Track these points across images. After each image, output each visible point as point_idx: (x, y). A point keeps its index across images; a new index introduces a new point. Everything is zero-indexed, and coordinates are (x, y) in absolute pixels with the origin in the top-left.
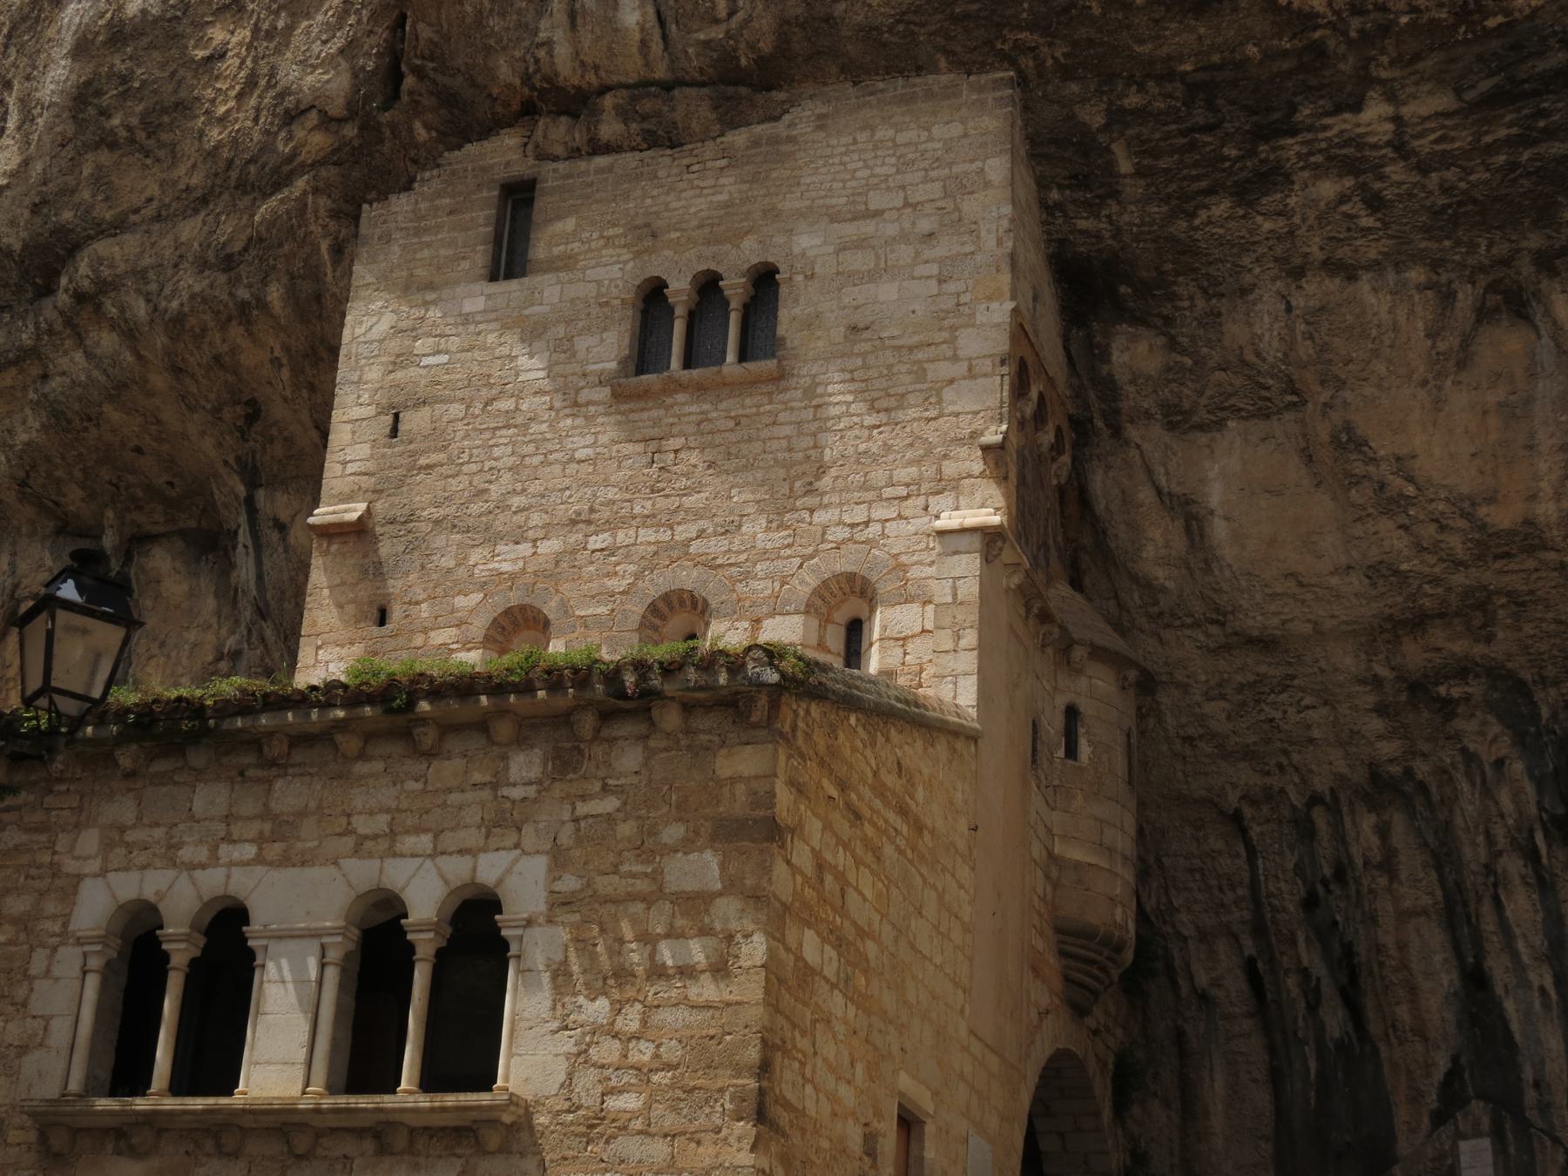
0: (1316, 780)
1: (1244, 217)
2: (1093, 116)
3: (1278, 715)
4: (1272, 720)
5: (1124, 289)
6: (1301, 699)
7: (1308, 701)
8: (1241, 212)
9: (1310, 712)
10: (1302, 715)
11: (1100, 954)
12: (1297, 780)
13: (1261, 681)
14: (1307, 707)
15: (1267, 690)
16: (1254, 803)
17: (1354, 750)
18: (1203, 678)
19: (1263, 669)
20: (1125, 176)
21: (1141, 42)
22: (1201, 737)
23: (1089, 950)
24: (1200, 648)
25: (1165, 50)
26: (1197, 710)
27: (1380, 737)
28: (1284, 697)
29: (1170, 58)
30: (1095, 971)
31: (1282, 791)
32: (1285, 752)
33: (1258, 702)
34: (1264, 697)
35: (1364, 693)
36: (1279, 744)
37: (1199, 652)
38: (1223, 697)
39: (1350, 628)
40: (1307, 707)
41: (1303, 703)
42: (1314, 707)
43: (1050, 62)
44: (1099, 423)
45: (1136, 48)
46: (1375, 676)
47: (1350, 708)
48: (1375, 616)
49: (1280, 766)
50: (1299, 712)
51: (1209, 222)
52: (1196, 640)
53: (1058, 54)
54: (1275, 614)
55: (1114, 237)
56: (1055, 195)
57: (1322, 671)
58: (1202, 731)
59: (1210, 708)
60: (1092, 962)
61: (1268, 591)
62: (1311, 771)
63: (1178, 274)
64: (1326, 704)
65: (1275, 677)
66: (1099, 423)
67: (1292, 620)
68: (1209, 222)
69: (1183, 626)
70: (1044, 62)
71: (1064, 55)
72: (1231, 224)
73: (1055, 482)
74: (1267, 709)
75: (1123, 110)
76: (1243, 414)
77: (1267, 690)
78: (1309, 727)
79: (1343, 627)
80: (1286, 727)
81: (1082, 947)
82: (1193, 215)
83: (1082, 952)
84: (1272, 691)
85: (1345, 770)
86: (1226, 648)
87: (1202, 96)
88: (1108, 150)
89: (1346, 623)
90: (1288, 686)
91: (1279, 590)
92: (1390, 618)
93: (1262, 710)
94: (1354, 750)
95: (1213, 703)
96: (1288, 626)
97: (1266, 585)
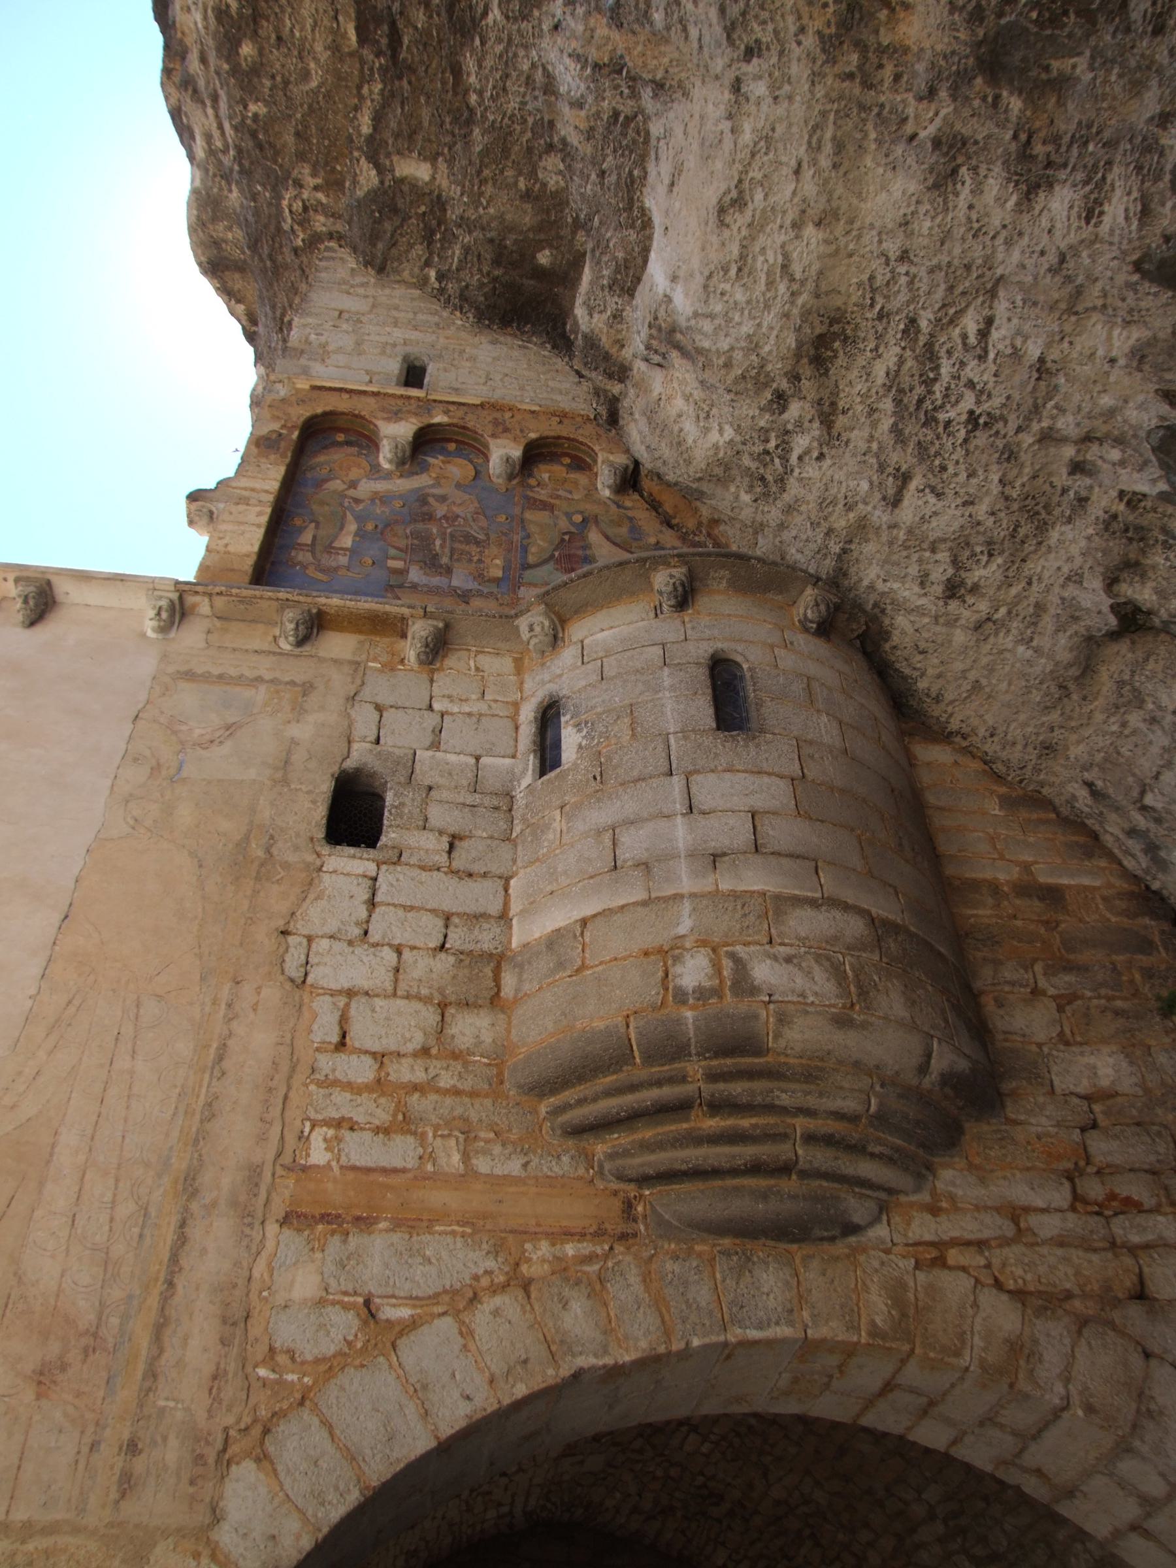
0: (1132, 414)
1: (483, 43)
2: (368, 177)
3: (969, 402)
4: (973, 418)
5: (544, 258)
6: (964, 337)
7: (971, 324)
8: (477, 42)
9: (995, 335)
10: (991, 356)
11: (683, 1079)
12: (1115, 454)
13: (901, 391)
14: (984, 334)
15: (920, 390)
16: (1131, 567)
17: (1096, 290)
18: (865, 485)
19: (880, 371)
20: (433, 178)
21: (306, 75)
22: (955, 562)
23: (633, 1088)
24: (821, 457)
25: (325, 56)
26: (902, 535)
27: (1091, 213)
28: (946, 369)
29: (335, 48)
30: (712, 1124)
31: (1133, 500)
32: (1048, 437)
33: (930, 421)
34: (927, 405)
35: (977, 191)
36: (1027, 439)
37: (828, 462)
38: (905, 478)
39: (828, 148)
40: (984, 334)
41: (972, 340)
42: (989, 321)
43: (321, 196)
44: (616, 388)
45: (314, 84)
46: (937, 143)
47: (1008, 243)
48: (816, 77)
49: (1077, 468)
50: (982, 358)
51: (480, 93)
52: (807, 452)
53: (311, 182)
54: (770, 284)
55: (470, 233)
56: (433, 274)
57: (904, 257)
58: (943, 556)
59: (907, 513)
60: (679, 1108)
61: (733, 272)
62: (1111, 413)
63: (533, 174)
64: (993, 294)
65: (901, 361)
66: (616, 388)
67: (786, 256)
68: (480, 93)
69: (785, 459)
70: (320, 203)
71: (314, 175)
72: (489, 63)
73: (607, 493)
74: (952, 414)
75: (370, 139)
76: (636, 173)
77: (920, 390)
78: (1016, 354)
79: (825, 162)
80: (997, 401)
81: (609, 1093)
82: (471, 111)
83: (629, 1100)
84: (929, 383)
85: (1137, 334)
86: (827, 414)
87: (372, 28)
88: (402, 180)
89: (815, 148)
90: (929, 346)
91: (735, 250)
92: (830, 45)
93: (948, 423)
94: (1096, 290)
95: (906, 503)
96: (797, 269)
97: (726, 270)
